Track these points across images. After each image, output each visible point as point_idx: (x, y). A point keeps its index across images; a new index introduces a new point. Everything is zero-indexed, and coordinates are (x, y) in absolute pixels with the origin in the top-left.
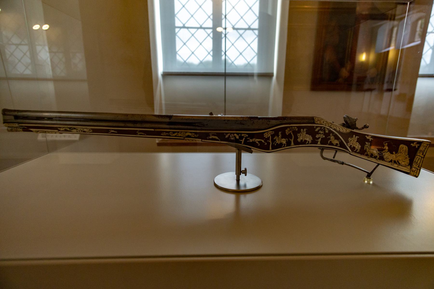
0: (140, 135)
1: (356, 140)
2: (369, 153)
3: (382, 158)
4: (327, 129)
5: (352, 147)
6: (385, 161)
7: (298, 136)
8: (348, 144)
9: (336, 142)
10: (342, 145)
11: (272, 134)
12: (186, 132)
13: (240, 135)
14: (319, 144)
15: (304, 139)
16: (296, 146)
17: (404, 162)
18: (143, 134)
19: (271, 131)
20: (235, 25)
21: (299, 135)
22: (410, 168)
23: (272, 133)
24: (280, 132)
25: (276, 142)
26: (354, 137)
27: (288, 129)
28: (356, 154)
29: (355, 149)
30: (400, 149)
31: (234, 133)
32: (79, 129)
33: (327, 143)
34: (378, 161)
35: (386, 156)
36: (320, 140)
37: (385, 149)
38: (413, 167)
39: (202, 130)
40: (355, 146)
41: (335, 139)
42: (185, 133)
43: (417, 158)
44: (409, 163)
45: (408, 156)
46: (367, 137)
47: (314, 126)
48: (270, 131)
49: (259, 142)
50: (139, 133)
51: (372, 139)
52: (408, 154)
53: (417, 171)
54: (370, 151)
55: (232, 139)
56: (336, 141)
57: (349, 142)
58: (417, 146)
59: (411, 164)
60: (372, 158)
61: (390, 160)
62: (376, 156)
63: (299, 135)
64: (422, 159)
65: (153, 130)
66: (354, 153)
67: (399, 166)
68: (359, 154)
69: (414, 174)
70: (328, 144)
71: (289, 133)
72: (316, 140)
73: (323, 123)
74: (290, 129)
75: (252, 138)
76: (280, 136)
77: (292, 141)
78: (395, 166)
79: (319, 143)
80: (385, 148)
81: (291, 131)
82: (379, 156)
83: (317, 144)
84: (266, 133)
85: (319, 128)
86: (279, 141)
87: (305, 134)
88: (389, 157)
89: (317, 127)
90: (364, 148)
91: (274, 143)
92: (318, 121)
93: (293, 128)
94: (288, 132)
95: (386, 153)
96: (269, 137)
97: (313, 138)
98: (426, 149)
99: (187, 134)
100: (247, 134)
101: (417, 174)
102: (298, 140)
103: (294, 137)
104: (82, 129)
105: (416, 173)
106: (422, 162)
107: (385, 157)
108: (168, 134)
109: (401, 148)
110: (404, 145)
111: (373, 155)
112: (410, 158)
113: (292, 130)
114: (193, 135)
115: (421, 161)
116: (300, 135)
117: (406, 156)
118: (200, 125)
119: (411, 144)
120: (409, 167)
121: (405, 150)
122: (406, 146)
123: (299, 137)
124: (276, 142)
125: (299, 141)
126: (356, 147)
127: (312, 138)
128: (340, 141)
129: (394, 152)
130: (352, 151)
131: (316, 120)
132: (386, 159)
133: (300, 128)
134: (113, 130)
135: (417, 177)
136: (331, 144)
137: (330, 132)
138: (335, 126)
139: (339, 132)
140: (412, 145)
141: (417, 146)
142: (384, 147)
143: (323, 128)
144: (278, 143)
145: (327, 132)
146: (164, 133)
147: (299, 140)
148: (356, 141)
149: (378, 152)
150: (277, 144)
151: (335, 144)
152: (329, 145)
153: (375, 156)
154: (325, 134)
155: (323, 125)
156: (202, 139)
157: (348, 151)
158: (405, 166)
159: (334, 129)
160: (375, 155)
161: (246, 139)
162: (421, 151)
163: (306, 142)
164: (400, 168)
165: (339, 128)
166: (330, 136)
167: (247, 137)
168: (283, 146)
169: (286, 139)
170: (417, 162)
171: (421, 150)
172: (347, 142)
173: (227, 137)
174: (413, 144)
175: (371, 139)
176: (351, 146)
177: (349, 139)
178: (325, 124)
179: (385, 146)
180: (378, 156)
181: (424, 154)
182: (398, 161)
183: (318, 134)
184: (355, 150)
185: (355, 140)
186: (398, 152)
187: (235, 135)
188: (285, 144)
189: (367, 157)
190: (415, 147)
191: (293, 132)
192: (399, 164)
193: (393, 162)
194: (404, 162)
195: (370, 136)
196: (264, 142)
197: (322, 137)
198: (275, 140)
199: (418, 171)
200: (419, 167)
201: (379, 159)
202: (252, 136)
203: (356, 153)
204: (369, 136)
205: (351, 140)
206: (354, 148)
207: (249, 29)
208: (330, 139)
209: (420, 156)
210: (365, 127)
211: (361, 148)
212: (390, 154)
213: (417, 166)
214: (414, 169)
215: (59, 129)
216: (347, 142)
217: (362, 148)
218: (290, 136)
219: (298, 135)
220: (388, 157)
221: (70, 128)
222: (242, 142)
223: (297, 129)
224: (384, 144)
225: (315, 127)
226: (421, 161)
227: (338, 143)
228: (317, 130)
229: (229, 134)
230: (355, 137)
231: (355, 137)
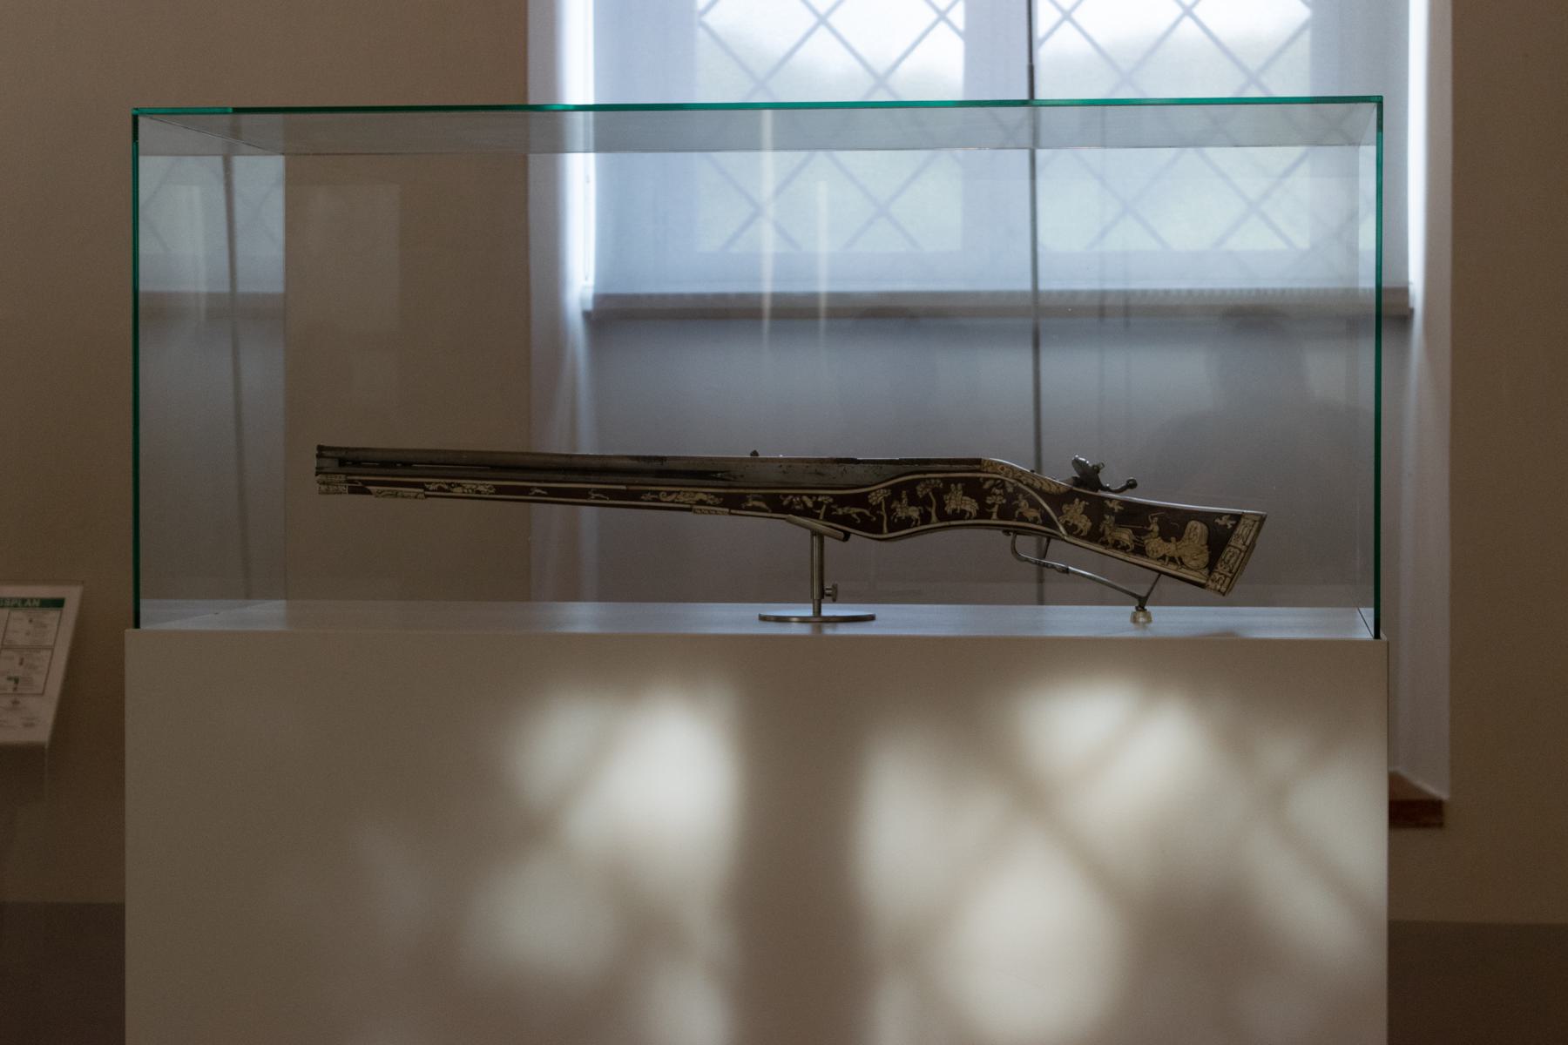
0: (597, 498)
1: (1082, 509)
2: (1109, 539)
3: (1140, 550)
4: (1012, 484)
9: (1032, 513)
10: (1047, 521)
12: (696, 493)
13: (814, 498)
14: (994, 520)
17: (1195, 559)
18: (602, 496)
19: (883, 488)
21: (948, 497)
30: (1187, 531)
31: (801, 495)
32: (468, 486)
33: (1014, 518)
35: (1153, 545)
36: (995, 509)
37: (1152, 531)
39: (729, 487)
40: (1076, 523)
42: (693, 494)
43: (1230, 551)
47: (979, 478)
49: (858, 514)
50: (594, 495)
51: (1120, 508)
52: (1208, 544)
53: (1224, 582)
55: (798, 507)
59: (1211, 566)
60: (1117, 549)
62: (1128, 546)
63: (946, 497)
64: (1242, 554)
65: (624, 487)
69: (1216, 586)
71: (924, 492)
72: (987, 510)
75: (842, 506)
76: (904, 501)
78: (1171, 569)
79: (994, 516)
80: (1151, 528)
83: (989, 518)
84: (873, 494)
85: (991, 482)
88: (1159, 549)
89: (986, 479)
90: (1099, 527)
91: (892, 518)
93: (933, 481)
96: (881, 503)
97: (979, 505)
99: (700, 496)
100: (831, 496)
103: (937, 502)
104: (474, 487)
106: (1240, 560)
108: (656, 497)
111: (1119, 544)
114: (711, 499)
115: (1238, 558)
116: (950, 499)
117: (1202, 548)
118: (727, 477)
120: (1206, 572)
123: (947, 502)
127: (976, 505)
129: (1173, 539)
130: (1068, 533)
131: (985, 464)
133: (947, 482)
134: (538, 488)
136: (1022, 518)
137: (1017, 490)
139: (1040, 492)
142: (1149, 526)
146: (649, 494)
147: (949, 510)
149: (1133, 537)
150: (899, 518)
154: (1006, 495)
155: (999, 474)
156: (731, 508)
157: (1061, 535)
159: (1027, 485)
161: (829, 510)
163: (965, 514)
165: (1042, 483)
166: (1017, 499)
167: (829, 505)
168: (914, 523)
170: (1229, 561)
172: (1060, 513)
173: (785, 503)
174: (1221, 519)
175: (1117, 508)
176: (1067, 522)
182: (1180, 559)
183: (990, 495)
184: (1078, 531)
187: (805, 498)
188: (917, 520)
190: (1226, 526)
192: (1182, 563)
193: (1167, 559)
194: (1195, 559)
195: (1117, 502)
197: (1000, 503)
198: (894, 510)
199: (1228, 580)
200: (1230, 572)
202: (841, 501)
206: (1075, 527)
208: (1019, 507)
209: (1235, 547)
210: (1131, 485)
211: (1092, 527)
212: (1161, 541)
214: (1218, 576)
215: (427, 486)
216: (1060, 513)
218: (925, 502)
221: (450, 484)
222: (819, 514)
223: (941, 485)
225: (981, 480)
226: (1238, 558)
227: (1039, 517)
228: (987, 486)
229: (790, 497)
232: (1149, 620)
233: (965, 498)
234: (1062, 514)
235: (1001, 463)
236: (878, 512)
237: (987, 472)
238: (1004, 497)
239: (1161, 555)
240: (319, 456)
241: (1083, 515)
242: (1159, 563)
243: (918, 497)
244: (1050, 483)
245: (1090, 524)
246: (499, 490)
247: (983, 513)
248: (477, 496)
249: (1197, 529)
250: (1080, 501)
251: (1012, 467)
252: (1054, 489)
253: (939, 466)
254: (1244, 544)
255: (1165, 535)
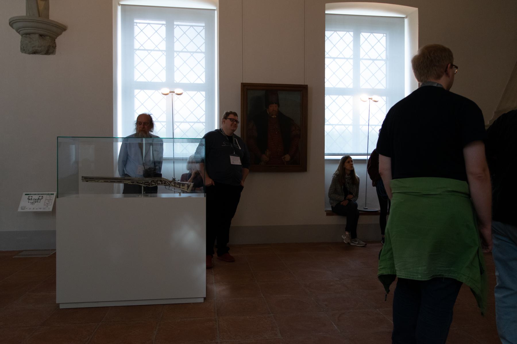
3: (180, 188)
9: (167, 184)
10: (169, 184)
20: (348, 86)
59: (188, 189)
133: (158, 180)
136: (166, 184)
137: (166, 181)
139: (169, 182)
154: (165, 182)
172: (171, 183)
216: (171, 183)
232: (181, 195)
240: (82, 177)
246: (105, 181)
247: (162, 183)
248: (102, 182)
249: (186, 185)
255: (183, 186)
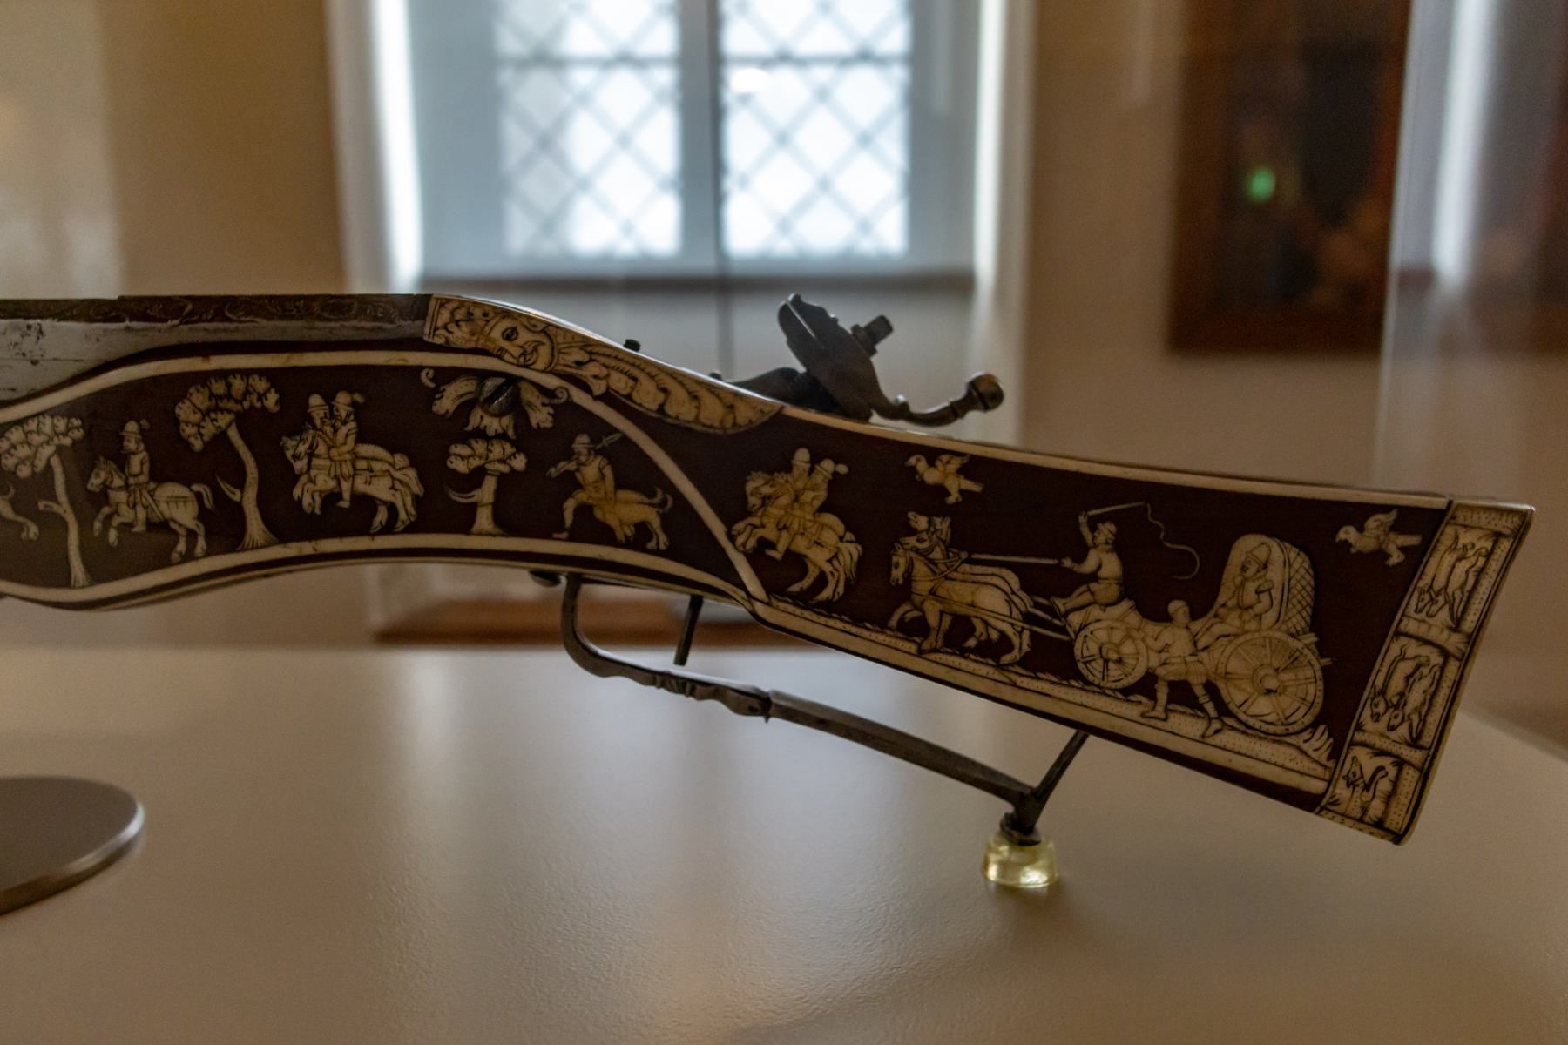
1: (822, 494)
5: (777, 555)
6: (1087, 682)
7: (296, 457)
8: (740, 526)
9: (630, 510)
11: (67, 441)
15: (346, 486)
16: (292, 550)
17: (1269, 692)
19: (53, 412)
21: (303, 448)
22: (1323, 756)
23: (65, 434)
24: (132, 427)
25: (109, 517)
26: (796, 472)
27: (199, 398)
28: (807, 614)
29: (801, 578)
34: (1019, 680)
35: (1102, 635)
36: (486, 492)
37: (1094, 577)
38: (1364, 744)
40: (801, 545)
41: (620, 484)
43: (1402, 657)
44: (1319, 700)
45: (1311, 638)
46: (922, 465)
47: (420, 368)
48: (42, 413)
51: (968, 485)
52: (1315, 625)
53: (1395, 784)
54: (941, 592)
56: (627, 502)
57: (749, 514)
58: (1402, 549)
60: (963, 653)
61: (1127, 681)
62: (1003, 634)
63: (294, 447)
64: (1453, 668)
66: (791, 608)
67: (1217, 732)
68: (831, 622)
69: (1364, 810)
70: (561, 529)
71: (209, 430)
72: (455, 497)
73: (506, 345)
74: (212, 395)
76: (135, 464)
77: (249, 499)
78: (1185, 729)
79: (484, 519)
80: (1089, 565)
81: (222, 410)
82: (1026, 635)
83: (466, 528)
86: (139, 508)
87: (351, 440)
88: (1128, 649)
89: (446, 376)
90: (888, 566)
91: (97, 525)
92: (457, 323)
94: (199, 426)
95: (1095, 612)
96: (49, 467)
97: (422, 479)
98: (1482, 571)
101: (1393, 809)
102: (297, 492)
105: (1389, 798)
107: (1093, 648)
109: (1244, 569)
110: (1274, 544)
112: (1326, 661)
113: (231, 405)
116: (311, 454)
117: (1295, 644)
119: (1342, 535)
120: (1319, 743)
121: (1287, 588)
122: (1293, 553)
123: (299, 465)
124: (117, 512)
125: (307, 501)
126: (810, 554)
127: (412, 474)
128: (663, 503)
130: (769, 590)
132: (1098, 665)
135: (1398, 838)
136: (590, 527)
137: (570, 418)
138: (627, 368)
139: (657, 425)
140: (1346, 544)
141: (1402, 549)
142: (1081, 557)
143: (491, 384)
144: (131, 525)
145: (541, 417)
147: (307, 495)
148: (817, 503)
149: (1024, 601)
150: (126, 527)
151: (629, 531)
152: (572, 538)
153: (989, 640)
154: (524, 438)
158: (1280, 729)
159: (609, 398)
160: (987, 624)
162: (1441, 599)
163: (374, 512)
164: (1232, 747)
165: (665, 391)
166: (569, 454)
168: (181, 546)
169: (196, 487)
171: (1437, 587)
172: (734, 510)
174: (1361, 529)
175: (956, 486)
176: (764, 544)
177: (750, 486)
178: (517, 352)
179: (1095, 546)
180: (1016, 641)
181: (1469, 623)
182: (1211, 689)
183: (464, 439)
184: (807, 583)
185: (808, 496)
186: (1220, 600)
188: (191, 534)
189: (913, 648)
190: (1381, 554)
191: (241, 420)
192: (1223, 710)
193: (1162, 694)
194: (1269, 692)
195: (956, 463)
196: (17, 511)
197: (504, 469)
199: (1410, 777)
200: (1414, 743)
201: (1024, 662)
203: (806, 608)
204: (945, 458)
205: (766, 490)
206: (797, 563)
207: (865, 57)
208: (579, 486)
212: (1134, 618)
213: (1393, 735)
214: (1368, 763)
216: (734, 510)
217: (874, 561)
219: (289, 454)
220: (1118, 646)
223: (272, 400)
224: (1085, 530)
227: (655, 522)
228: (446, 403)
230: (811, 471)
231: (811, 471)
233: (367, 450)
234: (746, 513)
235: (506, 314)
236: (41, 505)
237: (447, 348)
238: (519, 445)
239: (1138, 673)
241: (830, 519)
242: (1132, 711)
243: (187, 444)
244: (695, 390)
245: (852, 551)
250: (815, 460)
251: (548, 329)
252: (712, 413)
253: (265, 328)
254: (1456, 629)
